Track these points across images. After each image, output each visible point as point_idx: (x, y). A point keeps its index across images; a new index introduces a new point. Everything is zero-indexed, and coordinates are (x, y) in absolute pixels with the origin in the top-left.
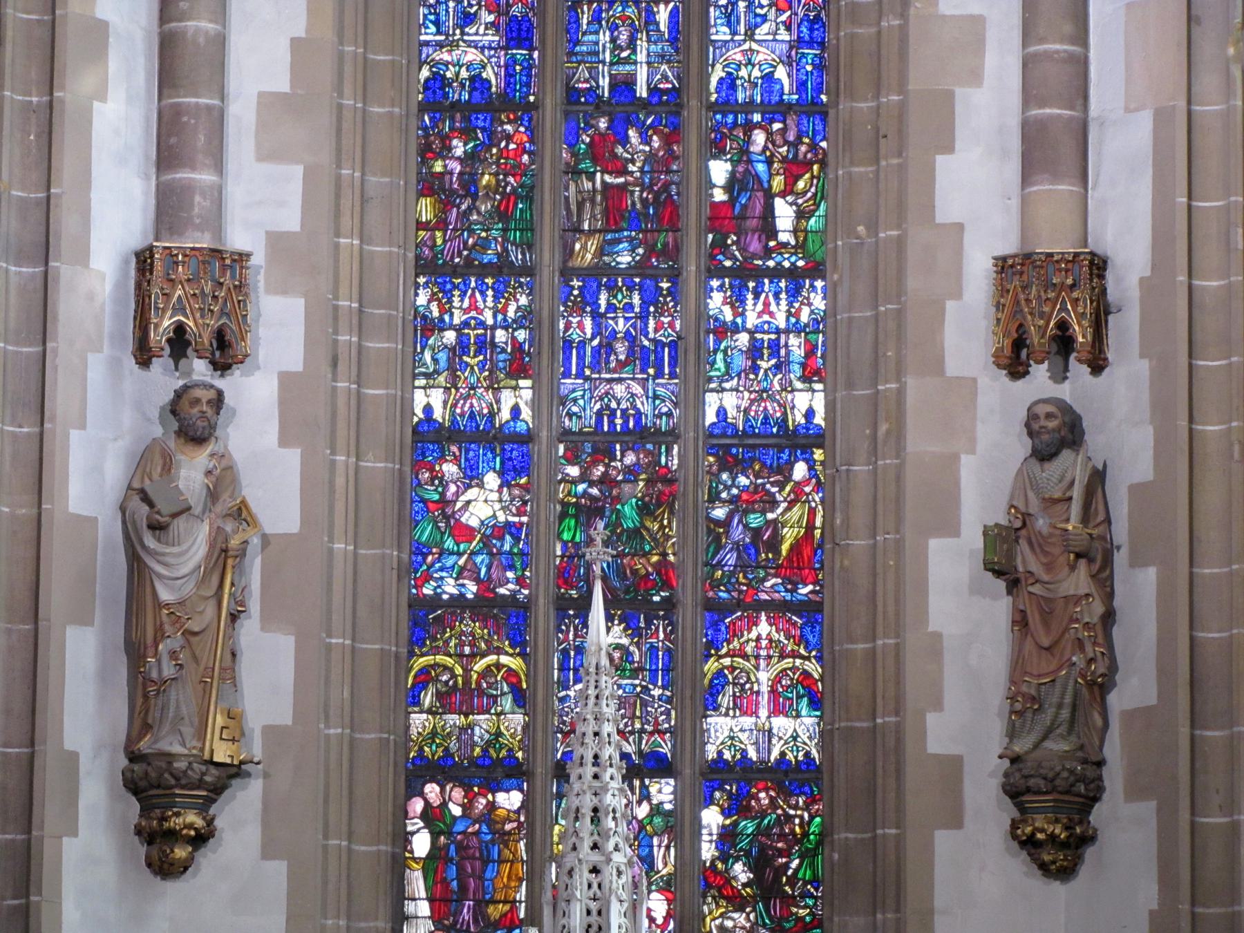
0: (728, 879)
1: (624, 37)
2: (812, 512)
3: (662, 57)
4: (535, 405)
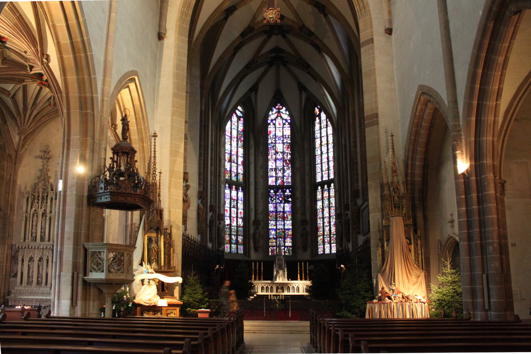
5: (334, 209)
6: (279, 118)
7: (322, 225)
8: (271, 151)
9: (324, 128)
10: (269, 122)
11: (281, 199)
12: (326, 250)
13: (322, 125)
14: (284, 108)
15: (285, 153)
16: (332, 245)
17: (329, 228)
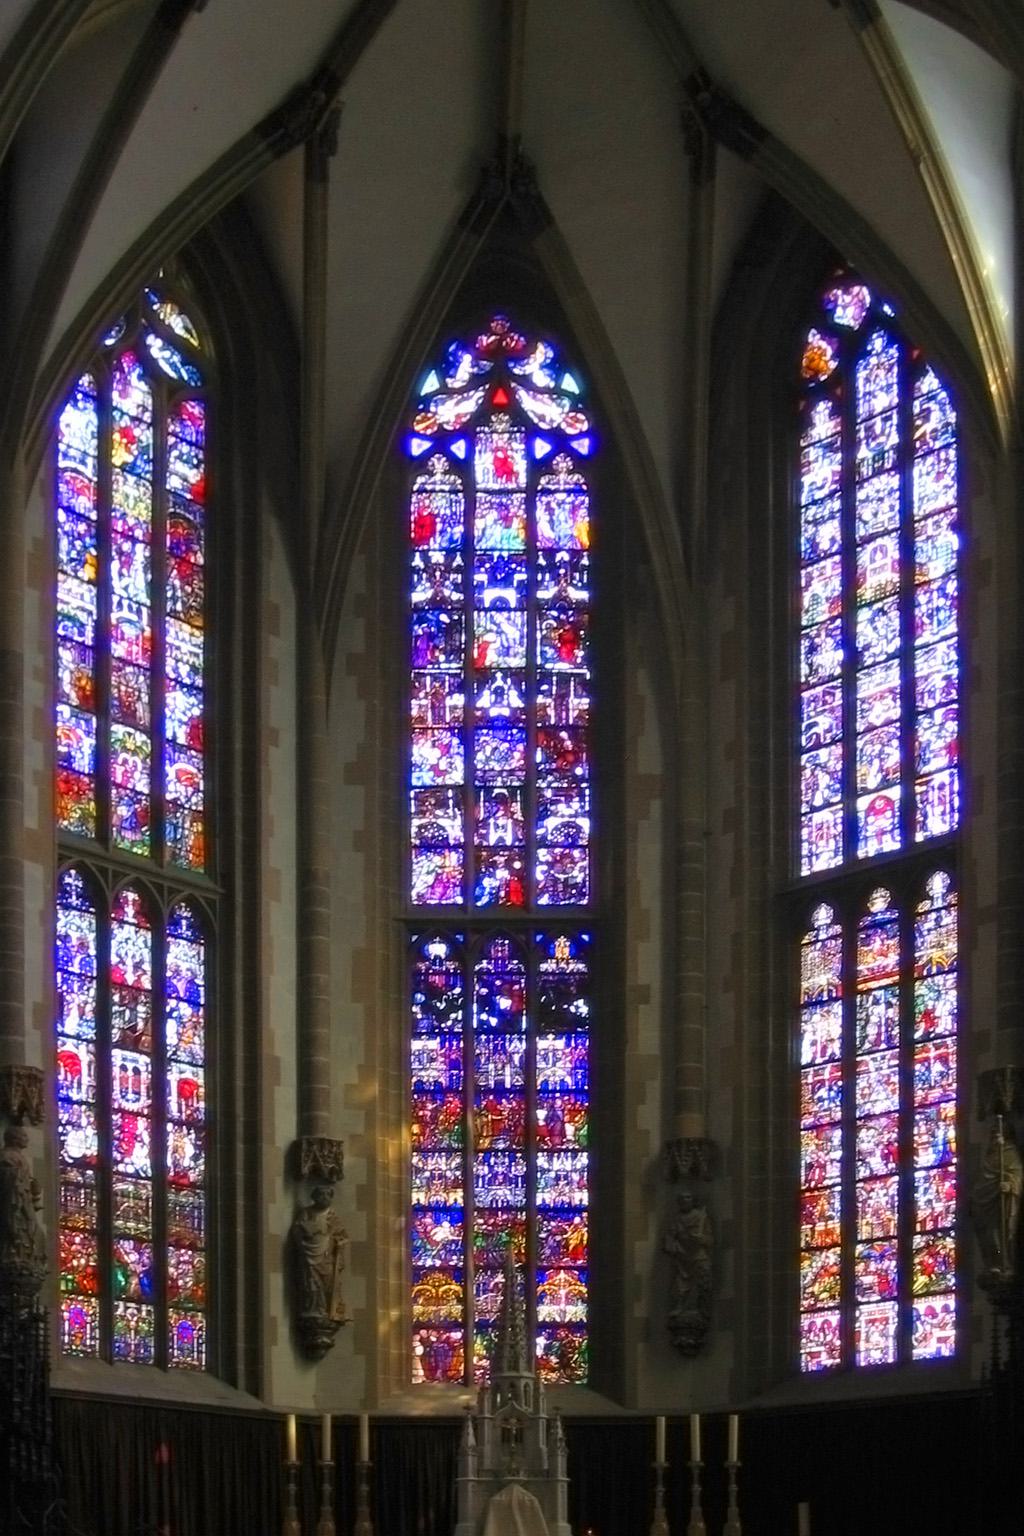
1: (500, 1066)
2: (583, 1235)
3: (516, 1073)
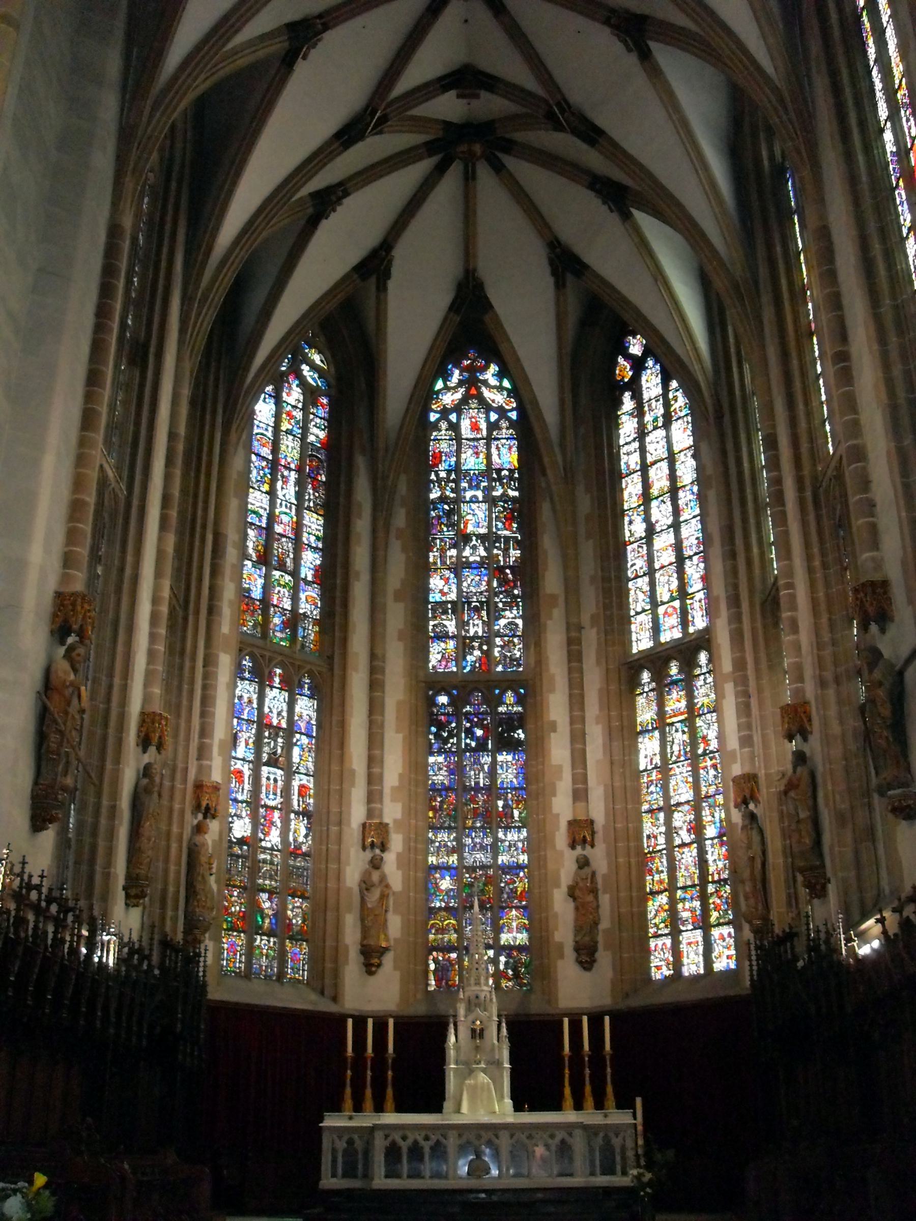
0: (507, 973)
4: (458, 860)
5: (714, 767)
6: (474, 403)
7: (662, 840)
8: (441, 531)
9: (655, 428)
10: (433, 417)
11: (479, 732)
12: (685, 961)
13: (648, 418)
14: (493, 368)
15: (498, 538)
16: (715, 933)
17: (695, 853)
